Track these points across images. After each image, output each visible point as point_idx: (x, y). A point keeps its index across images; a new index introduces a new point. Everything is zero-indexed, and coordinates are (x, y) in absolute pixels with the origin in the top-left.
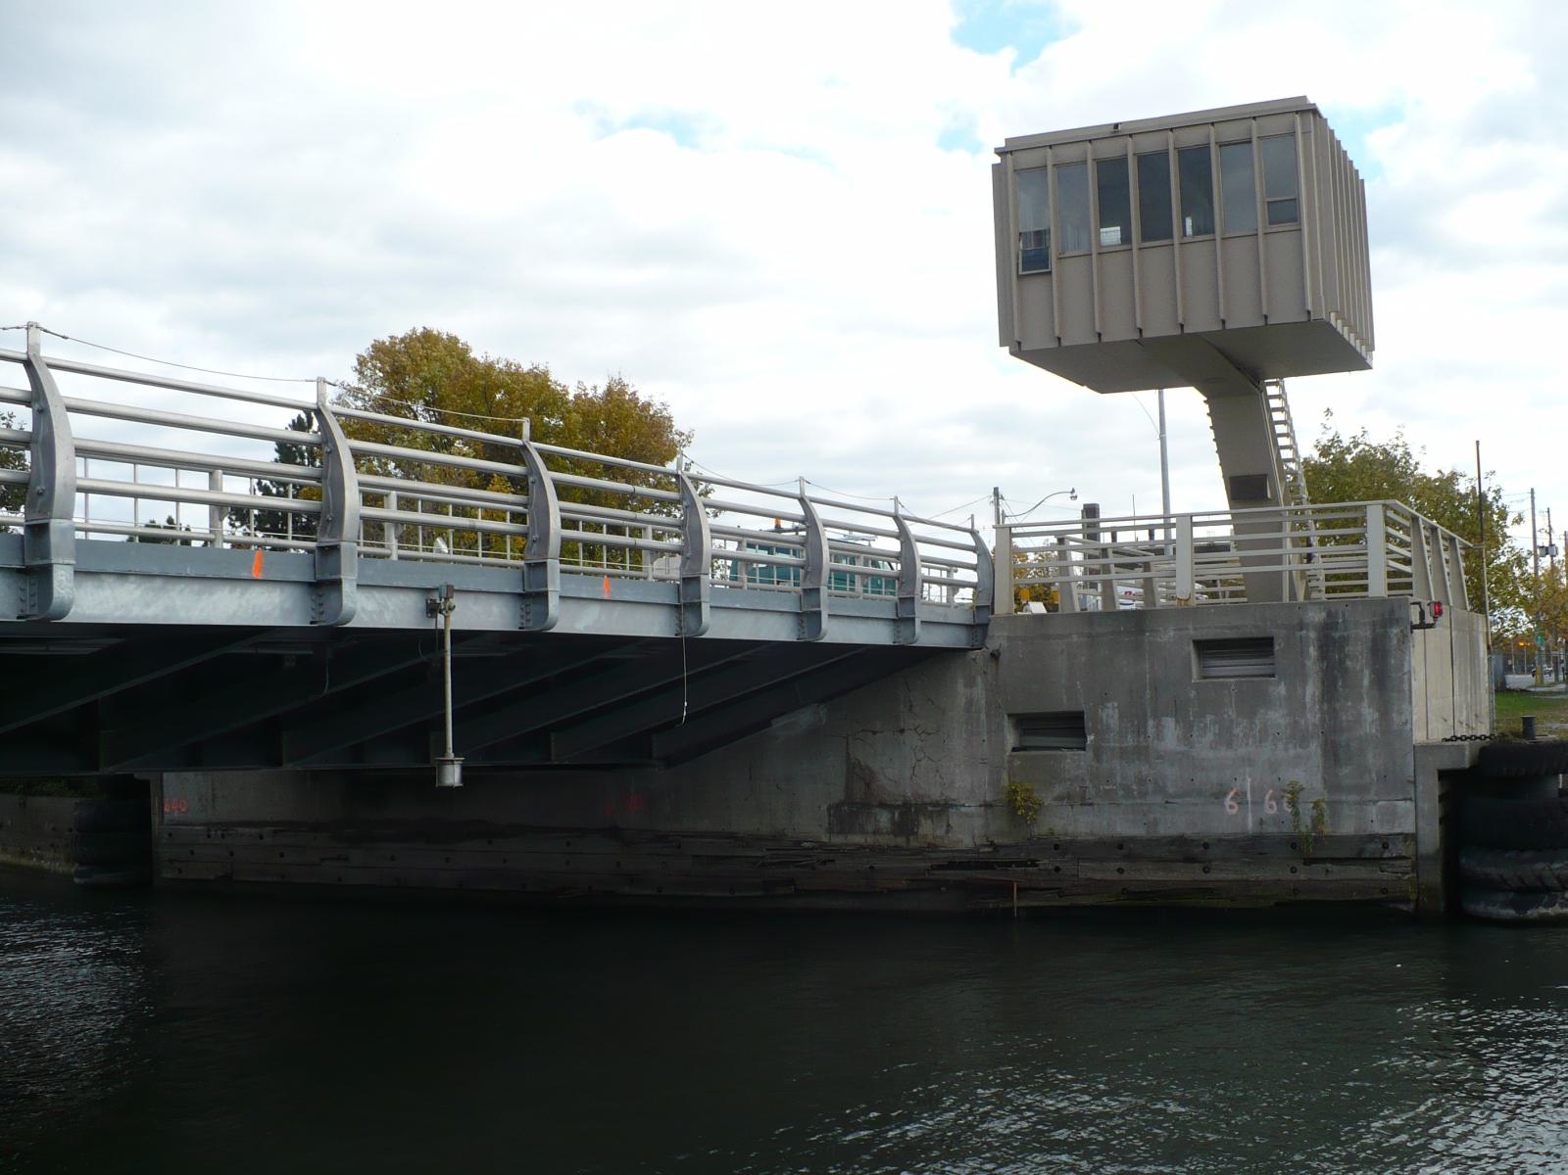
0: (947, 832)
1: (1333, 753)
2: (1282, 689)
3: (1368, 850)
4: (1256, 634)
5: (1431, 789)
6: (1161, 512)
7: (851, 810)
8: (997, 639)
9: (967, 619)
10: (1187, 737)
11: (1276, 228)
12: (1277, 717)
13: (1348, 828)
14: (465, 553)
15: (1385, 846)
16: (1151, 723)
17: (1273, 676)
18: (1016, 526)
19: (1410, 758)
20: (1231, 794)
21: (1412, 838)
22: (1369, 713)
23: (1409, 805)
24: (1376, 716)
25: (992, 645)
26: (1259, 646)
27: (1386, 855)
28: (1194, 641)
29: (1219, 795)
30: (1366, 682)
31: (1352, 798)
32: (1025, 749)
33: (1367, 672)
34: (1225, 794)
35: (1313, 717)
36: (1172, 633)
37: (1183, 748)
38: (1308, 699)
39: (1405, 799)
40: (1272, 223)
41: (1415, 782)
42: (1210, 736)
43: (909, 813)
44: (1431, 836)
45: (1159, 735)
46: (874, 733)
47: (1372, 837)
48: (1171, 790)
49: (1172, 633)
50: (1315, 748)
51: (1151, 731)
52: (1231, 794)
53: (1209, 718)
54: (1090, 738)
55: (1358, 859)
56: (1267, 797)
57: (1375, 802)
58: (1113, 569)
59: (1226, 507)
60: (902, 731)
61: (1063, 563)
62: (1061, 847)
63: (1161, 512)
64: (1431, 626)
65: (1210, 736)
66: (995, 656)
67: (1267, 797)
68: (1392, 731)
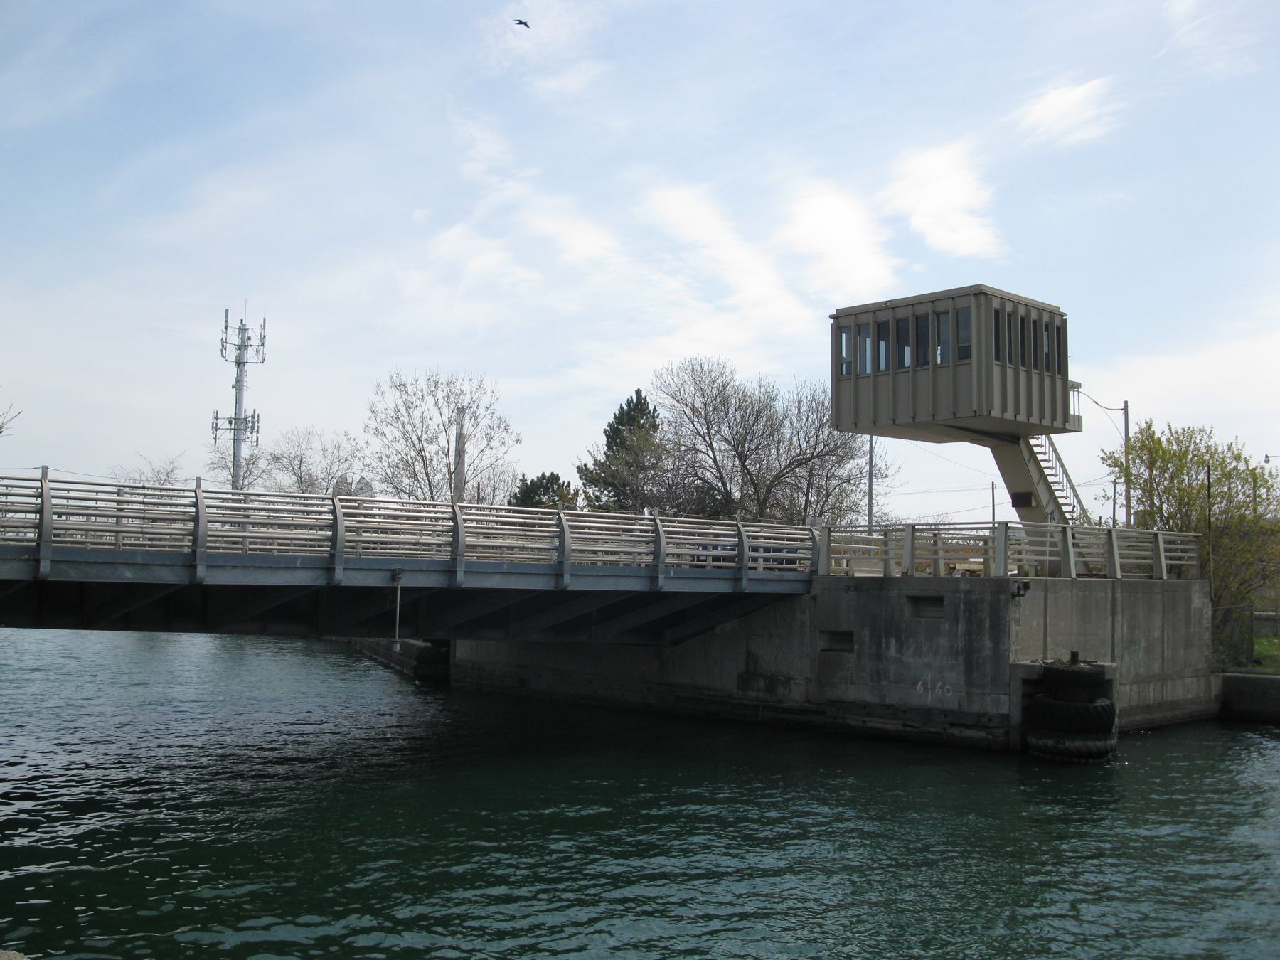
0: (790, 692)
1: (971, 666)
2: (947, 626)
3: (978, 721)
4: (936, 595)
5: (1017, 688)
6: (991, 521)
7: (746, 679)
8: (816, 590)
9: (806, 578)
10: (900, 651)
11: (961, 362)
12: (943, 641)
13: (976, 708)
14: (520, 530)
15: (990, 720)
16: (884, 641)
17: (941, 618)
18: (918, 525)
19: (1008, 671)
20: (920, 683)
21: (1006, 717)
22: (988, 643)
23: (1006, 697)
24: (992, 645)
25: (813, 592)
26: (937, 601)
27: (991, 725)
28: (907, 596)
29: (915, 684)
30: (988, 625)
31: (979, 691)
32: (831, 650)
33: (988, 620)
34: (918, 683)
35: (960, 644)
36: (896, 591)
37: (898, 656)
38: (959, 633)
39: (1004, 694)
40: (960, 359)
41: (1009, 685)
42: (911, 651)
43: (772, 682)
44: (1016, 717)
45: (888, 648)
46: (760, 636)
47: (985, 714)
48: (892, 679)
49: (896, 591)
50: (961, 659)
51: (884, 645)
52: (920, 683)
53: (911, 640)
54: (856, 647)
55: (976, 726)
56: (938, 686)
57: (989, 695)
58: (1024, 552)
59: (1019, 521)
60: (771, 636)
61: (935, 548)
62: (840, 704)
63: (991, 521)
64: (1023, 595)
65: (911, 651)
66: (814, 598)
67: (938, 686)
68: (999, 654)
